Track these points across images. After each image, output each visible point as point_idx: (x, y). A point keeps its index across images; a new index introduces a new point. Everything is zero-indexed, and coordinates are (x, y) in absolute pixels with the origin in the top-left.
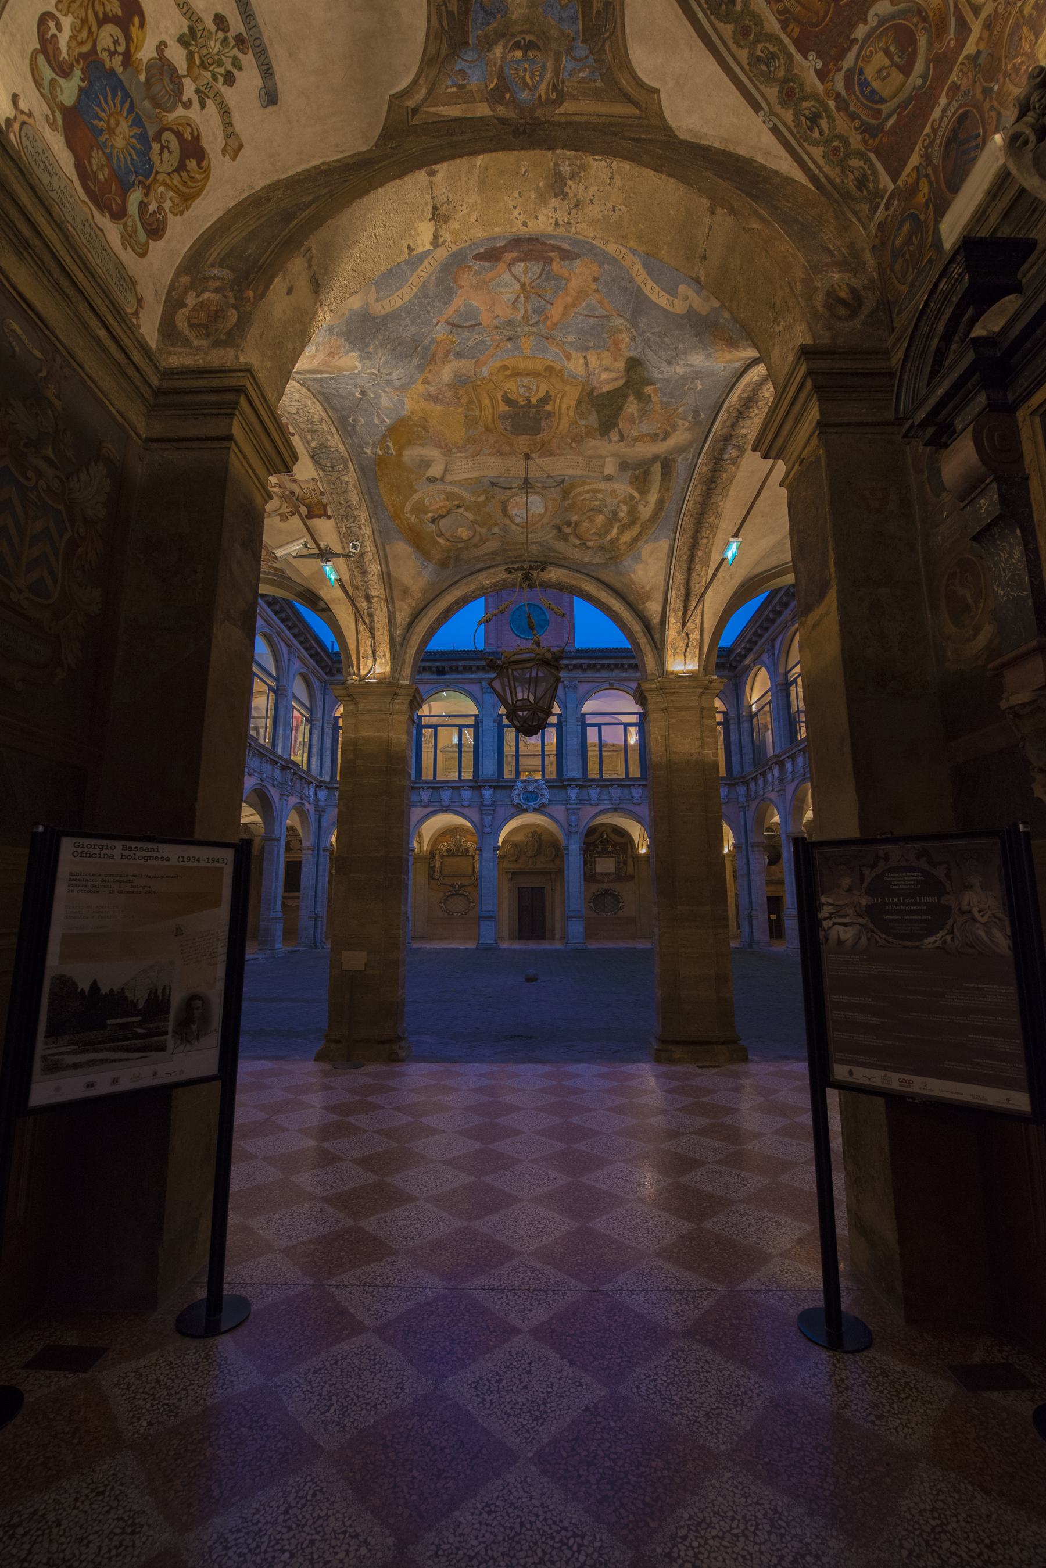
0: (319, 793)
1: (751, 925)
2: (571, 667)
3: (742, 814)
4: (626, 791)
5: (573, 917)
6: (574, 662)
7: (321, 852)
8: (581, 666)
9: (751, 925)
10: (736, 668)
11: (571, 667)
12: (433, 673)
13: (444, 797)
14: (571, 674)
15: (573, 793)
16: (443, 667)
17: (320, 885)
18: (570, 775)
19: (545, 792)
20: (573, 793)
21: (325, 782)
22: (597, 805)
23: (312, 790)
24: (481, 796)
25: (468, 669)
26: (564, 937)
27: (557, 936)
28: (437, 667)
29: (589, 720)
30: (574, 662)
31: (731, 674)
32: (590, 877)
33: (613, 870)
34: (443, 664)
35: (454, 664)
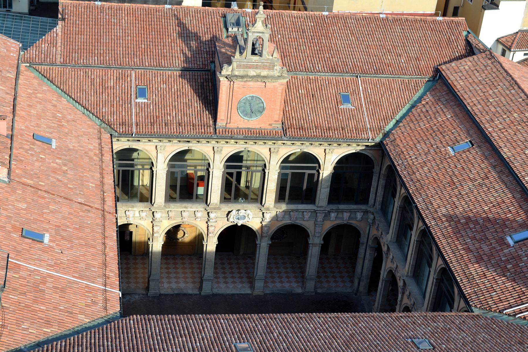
3: (368, 228)
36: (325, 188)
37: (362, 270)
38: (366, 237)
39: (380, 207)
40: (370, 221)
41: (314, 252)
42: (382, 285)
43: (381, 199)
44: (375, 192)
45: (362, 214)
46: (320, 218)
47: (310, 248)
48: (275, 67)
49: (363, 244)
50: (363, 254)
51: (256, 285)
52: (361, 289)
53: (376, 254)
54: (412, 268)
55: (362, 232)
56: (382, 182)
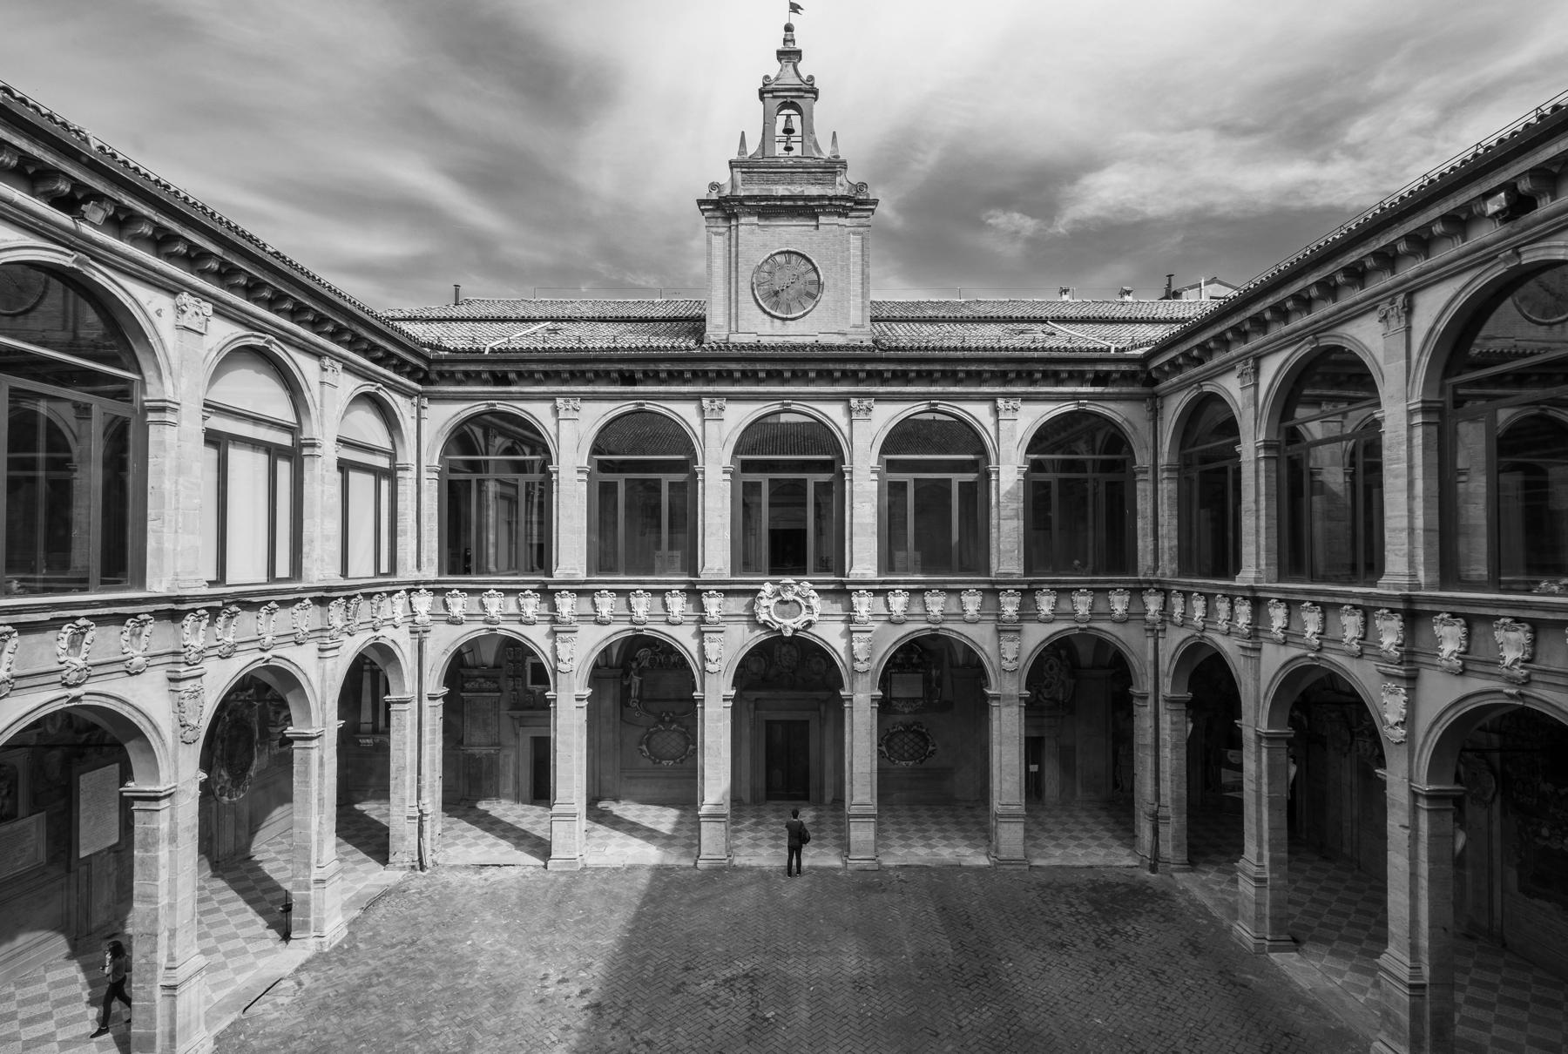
2: (862, 375)
3: (1151, 642)
4: (954, 599)
5: (856, 816)
6: (868, 367)
7: (426, 703)
8: (880, 373)
11: (862, 375)
12: (614, 382)
16: (632, 372)
27: (828, 798)
28: (621, 372)
30: (868, 367)
31: (1146, 390)
33: (920, 694)
34: (632, 367)
35: (652, 367)
36: (1010, 518)
38: (1150, 672)
39: (1175, 566)
42: (1259, 760)
43: (1175, 542)
44: (1150, 527)
45: (1127, 598)
47: (995, 713)
48: (838, 179)
49: (1144, 698)
50: (1151, 730)
51: (853, 834)
52: (1167, 850)
53: (1190, 726)
54: (1427, 544)
55: (1133, 659)
56: (1167, 488)
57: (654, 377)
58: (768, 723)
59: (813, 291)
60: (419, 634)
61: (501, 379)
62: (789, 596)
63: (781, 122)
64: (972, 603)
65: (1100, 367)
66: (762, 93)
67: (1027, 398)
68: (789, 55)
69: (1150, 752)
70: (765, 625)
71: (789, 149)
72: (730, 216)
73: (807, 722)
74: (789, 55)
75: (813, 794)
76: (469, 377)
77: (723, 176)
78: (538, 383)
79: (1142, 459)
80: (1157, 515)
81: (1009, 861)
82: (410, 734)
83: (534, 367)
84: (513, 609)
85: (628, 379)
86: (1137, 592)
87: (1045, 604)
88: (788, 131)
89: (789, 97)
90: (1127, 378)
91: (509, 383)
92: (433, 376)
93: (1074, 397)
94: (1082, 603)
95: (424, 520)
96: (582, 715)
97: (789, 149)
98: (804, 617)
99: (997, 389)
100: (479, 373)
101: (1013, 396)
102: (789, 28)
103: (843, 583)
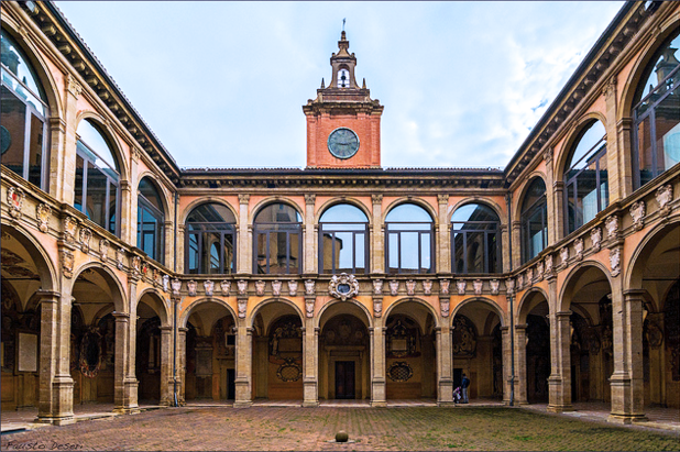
0: (173, 284)
1: (512, 389)
4: (419, 285)
7: (177, 332)
9: (512, 389)
10: (510, 184)
13: (275, 289)
14: (377, 189)
15: (378, 286)
17: (178, 358)
18: (375, 271)
19: (355, 285)
20: (378, 286)
21: (178, 276)
22: (396, 295)
23: (166, 281)
24: (305, 288)
25: (292, 183)
26: (369, 398)
27: (364, 397)
29: (391, 227)
32: (389, 354)
37: (513, 367)
40: (510, 291)
41: (444, 341)
46: (445, 287)
57: (282, 183)
58: (337, 363)
59: (354, 146)
60: (175, 299)
61: (213, 185)
62: (344, 282)
63: (340, 74)
64: (428, 287)
65: (484, 178)
66: (331, 59)
67: (452, 194)
68: (344, 44)
69: (509, 353)
70: (333, 296)
71: (343, 85)
72: (318, 114)
73: (354, 362)
74: (344, 44)
75: (357, 395)
76: (200, 183)
77: (314, 97)
78: (231, 186)
79: (504, 222)
80: (510, 250)
81: (445, 402)
82: (170, 344)
83: (228, 178)
84: (218, 289)
85: (271, 185)
86: (502, 281)
87: (461, 286)
88: (343, 78)
89: (343, 60)
90: (496, 184)
91: (216, 186)
92: (182, 182)
93: (473, 193)
94: (478, 286)
95: (178, 250)
96: (250, 339)
97: (343, 85)
98: (352, 291)
99: (439, 189)
100: (203, 181)
101: (445, 192)
102: (343, 33)
103: (369, 276)
